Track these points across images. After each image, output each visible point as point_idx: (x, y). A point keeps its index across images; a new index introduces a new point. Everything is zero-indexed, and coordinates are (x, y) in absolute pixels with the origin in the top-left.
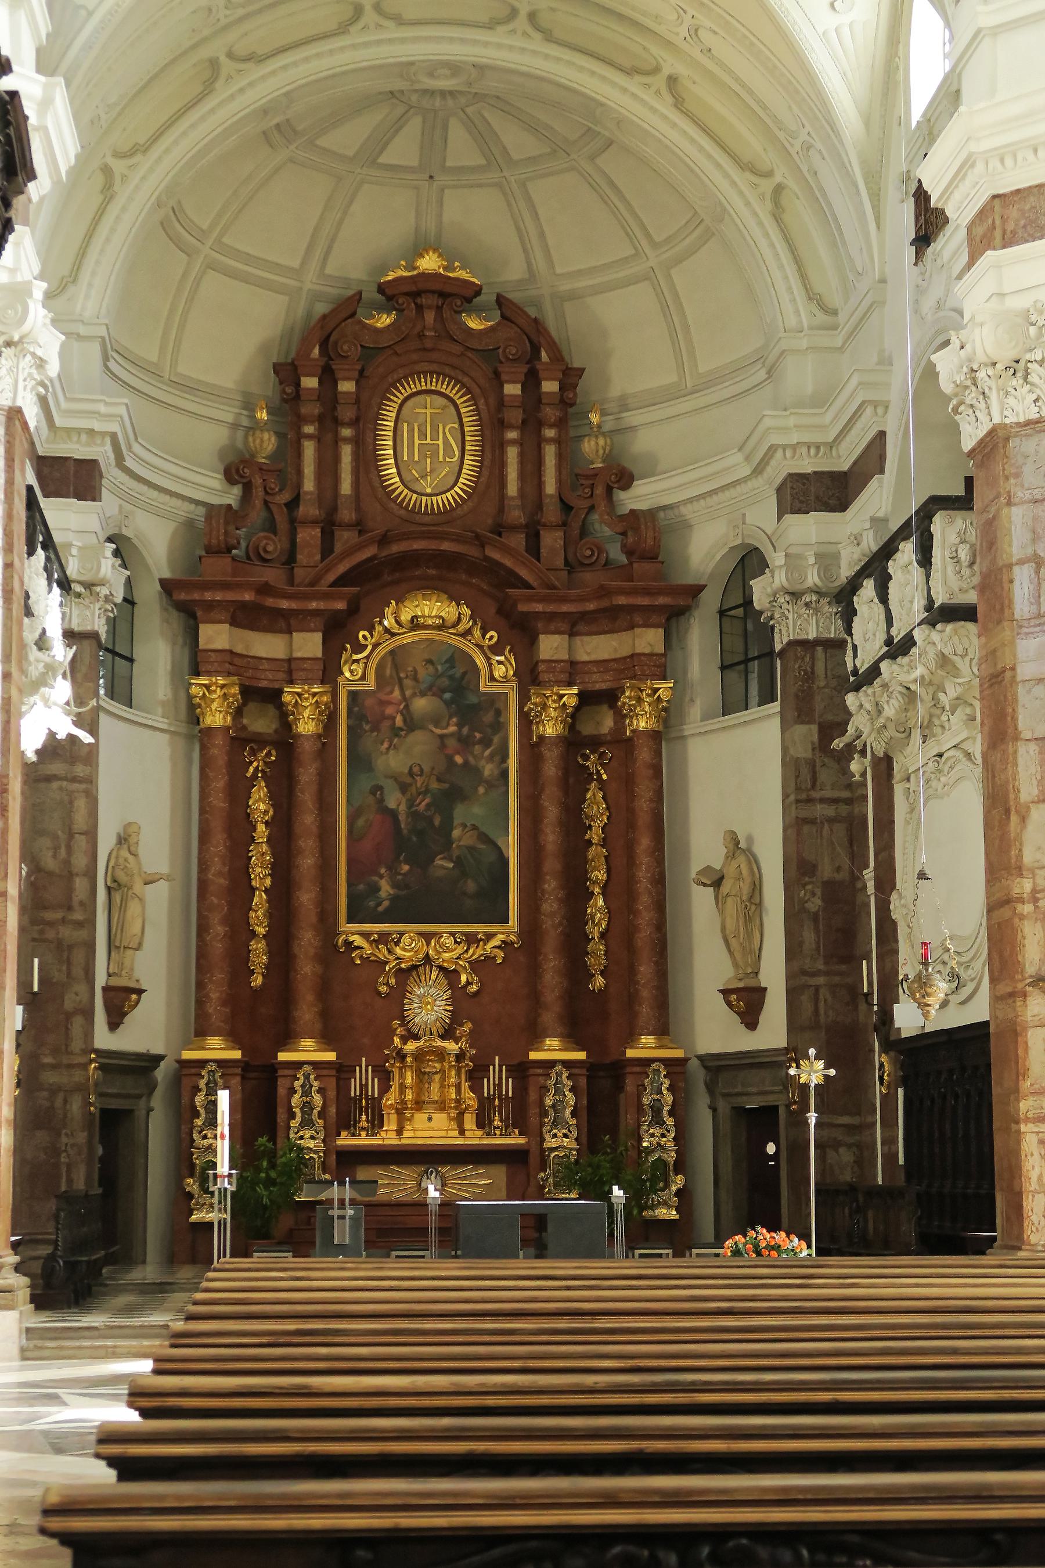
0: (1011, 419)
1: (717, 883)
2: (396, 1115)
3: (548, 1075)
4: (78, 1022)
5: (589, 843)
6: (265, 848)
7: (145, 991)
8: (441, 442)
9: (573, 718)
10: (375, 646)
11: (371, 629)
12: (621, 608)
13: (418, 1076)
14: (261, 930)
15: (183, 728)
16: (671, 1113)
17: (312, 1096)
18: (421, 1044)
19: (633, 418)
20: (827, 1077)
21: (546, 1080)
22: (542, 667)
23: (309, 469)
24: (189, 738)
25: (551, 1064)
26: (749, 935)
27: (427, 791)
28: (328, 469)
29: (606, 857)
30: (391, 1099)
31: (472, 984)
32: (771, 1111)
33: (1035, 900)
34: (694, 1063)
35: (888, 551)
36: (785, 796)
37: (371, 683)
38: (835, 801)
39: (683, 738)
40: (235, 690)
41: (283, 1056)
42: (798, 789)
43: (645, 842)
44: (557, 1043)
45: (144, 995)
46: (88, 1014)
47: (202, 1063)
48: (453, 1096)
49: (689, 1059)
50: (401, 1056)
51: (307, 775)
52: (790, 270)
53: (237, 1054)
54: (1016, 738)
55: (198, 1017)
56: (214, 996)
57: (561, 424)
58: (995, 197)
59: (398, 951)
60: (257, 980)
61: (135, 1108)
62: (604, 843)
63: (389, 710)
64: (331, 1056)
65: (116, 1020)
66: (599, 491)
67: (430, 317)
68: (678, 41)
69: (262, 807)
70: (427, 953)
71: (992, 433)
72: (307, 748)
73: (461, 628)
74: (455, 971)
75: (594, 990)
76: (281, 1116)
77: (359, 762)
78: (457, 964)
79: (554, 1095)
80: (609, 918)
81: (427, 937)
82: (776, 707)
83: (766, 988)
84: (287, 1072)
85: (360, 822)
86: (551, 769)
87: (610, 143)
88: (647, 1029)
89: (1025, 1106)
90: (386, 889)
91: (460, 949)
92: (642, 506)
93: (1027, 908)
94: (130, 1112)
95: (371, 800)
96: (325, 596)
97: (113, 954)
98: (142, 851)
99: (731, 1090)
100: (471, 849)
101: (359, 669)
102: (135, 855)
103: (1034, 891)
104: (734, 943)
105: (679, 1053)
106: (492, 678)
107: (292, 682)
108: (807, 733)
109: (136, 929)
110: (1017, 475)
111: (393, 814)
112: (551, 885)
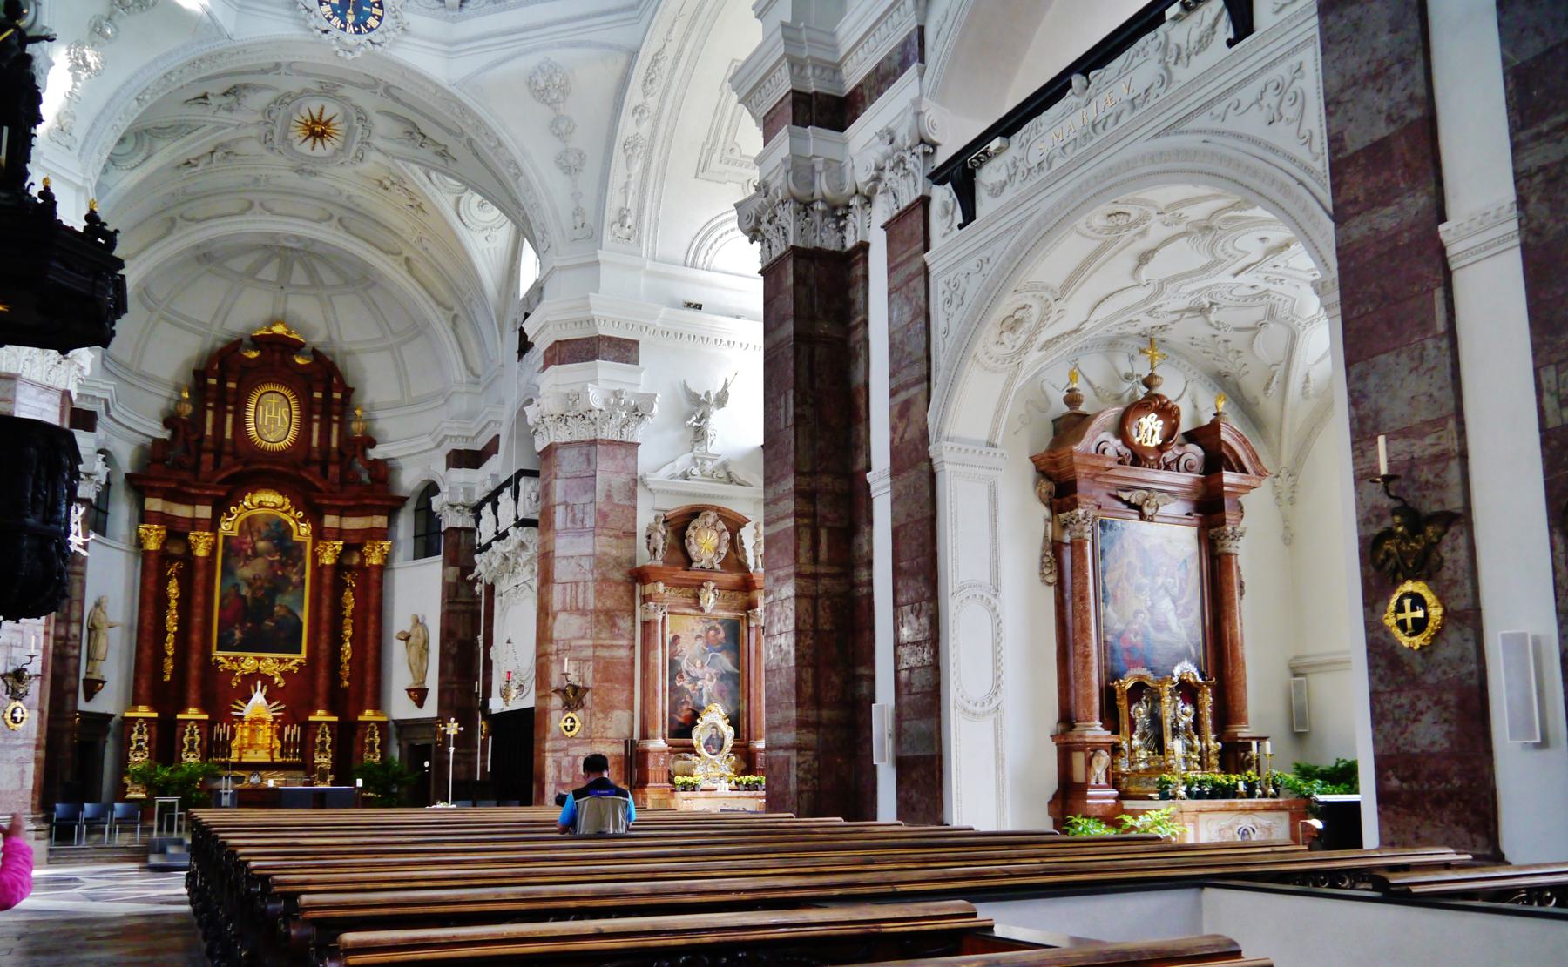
0: (558, 441)
1: (407, 639)
4: (70, 696)
5: (344, 617)
6: (174, 612)
8: (279, 417)
9: (340, 557)
10: (239, 514)
11: (237, 506)
12: (366, 505)
14: (170, 653)
15: (132, 549)
16: (379, 747)
19: (378, 414)
20: (459, 731)
22: (325, 531)
23: (209, 424)
24: (136, 554)
25: (319, 723)
26: (422, 665)
27: (261, 588)
28: (219, 425)
29: (353, 625)
32: (428, 746)
33: (558, 655)
35: (499, 491)
36: (443, 599)
37: (235, 533)
38: (467, 603)
39: (393, 569)
40: (163, 532)
41: (179, 716)
42: (449, 597)
43: (372, 618)
46: (76, 693)
47: (137, 718)
51: (200, 576)
52: (459, 354)
53: (155, 715)
54: (553, 582)
56: (144, 685)
57: (342, 414)
58: (557, 342)
60: (168, 678)
62: (351, 617)
63: (244, 547)
64: (206, 717)
65: (89, 696)
66: (359, 447)
67: (277, 356)
68: (412, 242)
69: (174, 591)
71: (550, 446)
72: (201, 562)
73: (284, 509)
76: (178, 747)
77: (228, 571)
81: (259, 659)
82: (440, 557)
85: (226, 602)
86: (327, 581)
87: (374, 284)
89: (548, 745)
90: (238, 634)
92: (378, 456)
93: (554, 658)
95: (233, 590)
96: (215, 489)
98: (108, 611)
100: (283, 617)
101: (230, 526)
102: (104, 613)
103: (557, 650)
104: (414, 667)
105: (384, 719)
106: (299, 534)
107: (194, 530)
108: (453, 572)
109: (102, 649)
110: (560, 466)
111: (244, 598)
112: (324, 636)
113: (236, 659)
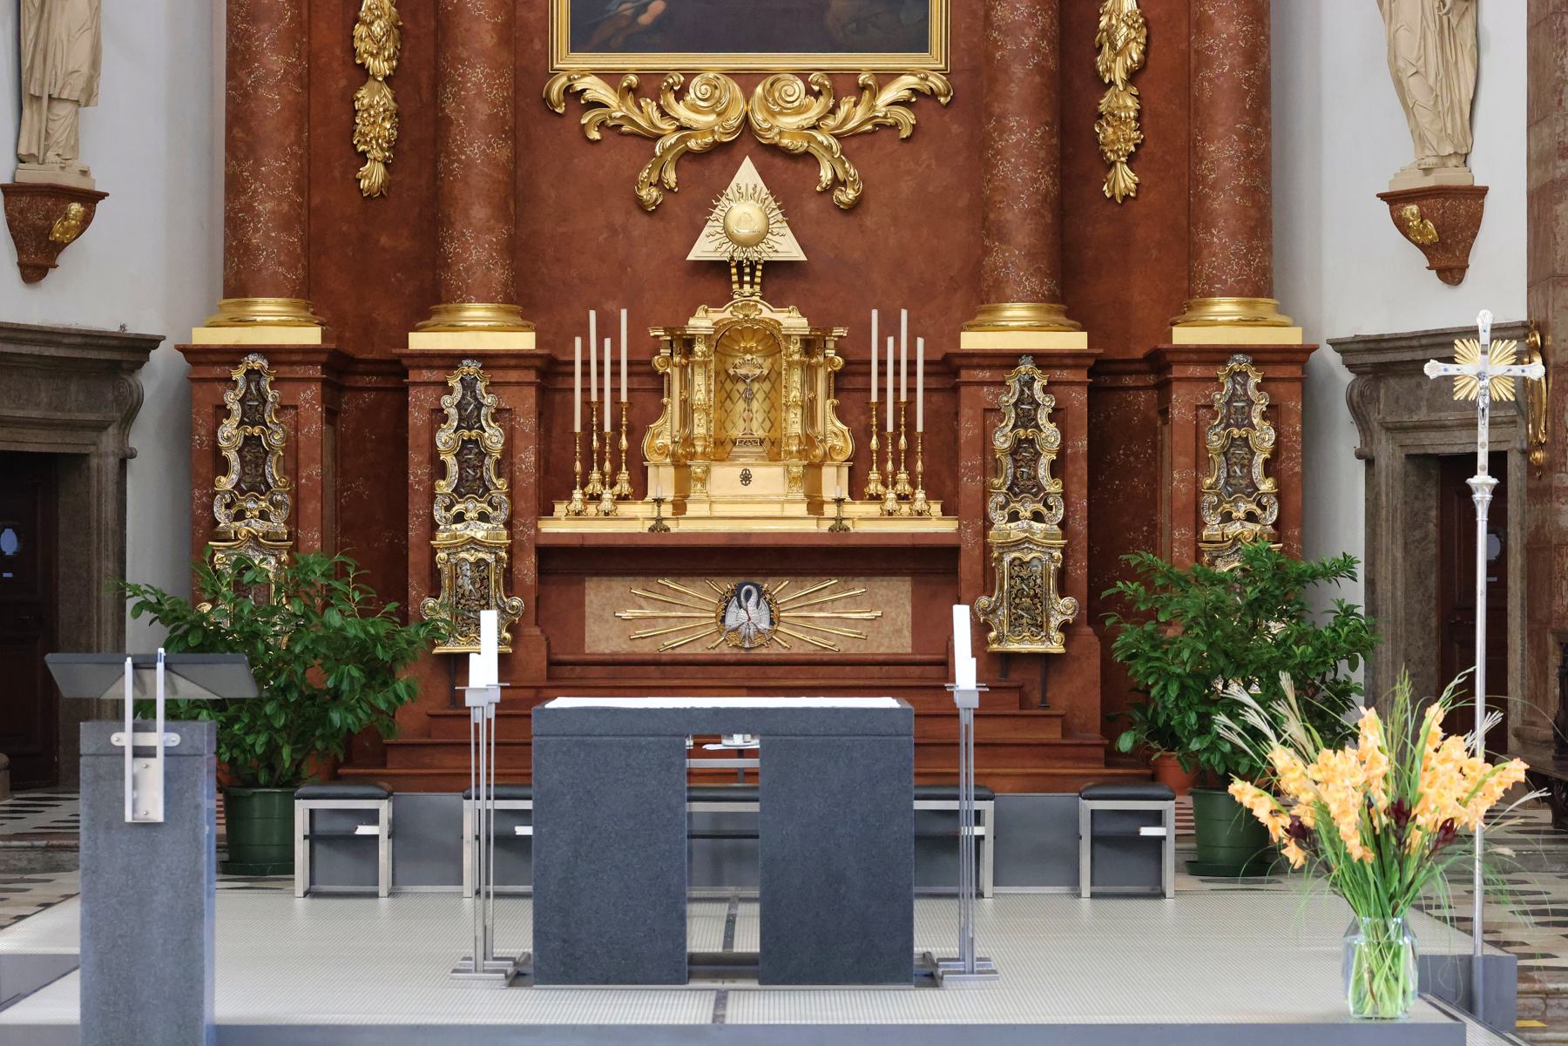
2: (672, 470)
3: (1002, 383)
7: (102, 196)
13: (720, 385)
14: (380, 66)
16: (1269, 468)
17: (481, 428)
18: (727, 314)
21: (997, 396)
25: (1009, 360)
30: (662, 435)
31: (844, 184)
34: (1331, 359)
41: (419, 341)
44: (1024, 313)
45: (100, 205)
47: (236, 354)
48: (796, 429)
49: (1314, 349)
50: (688, 344)
53: (311, 336)
55: (228, 250)
59: (681, 111)
61: (92, 449)
70: (746, 120)
74: (808, 158)
75: (1113, 197)
76: (418, 470)
78: (811, 139)
79: (1015, 426)
80: (1148, 38)
83: (1482, 192)
84: (426, 375)
88: (1220, 281)
91: (817, 107)
94: (77, 461)
97: (26, 112)
99: (1406, 418)
104: (1414, 85)
105: (1291, 337)
113: (647, 87)
